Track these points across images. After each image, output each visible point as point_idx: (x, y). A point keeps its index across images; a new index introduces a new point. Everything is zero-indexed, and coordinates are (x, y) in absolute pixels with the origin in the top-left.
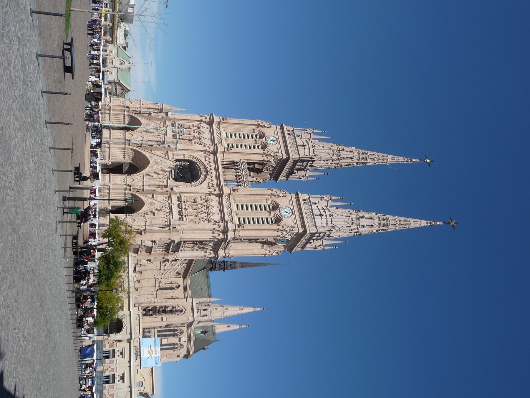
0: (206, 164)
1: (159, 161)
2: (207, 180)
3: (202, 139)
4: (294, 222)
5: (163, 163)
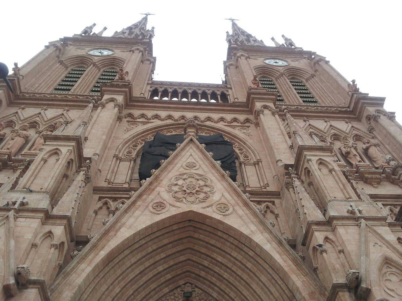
1: (180, 182)
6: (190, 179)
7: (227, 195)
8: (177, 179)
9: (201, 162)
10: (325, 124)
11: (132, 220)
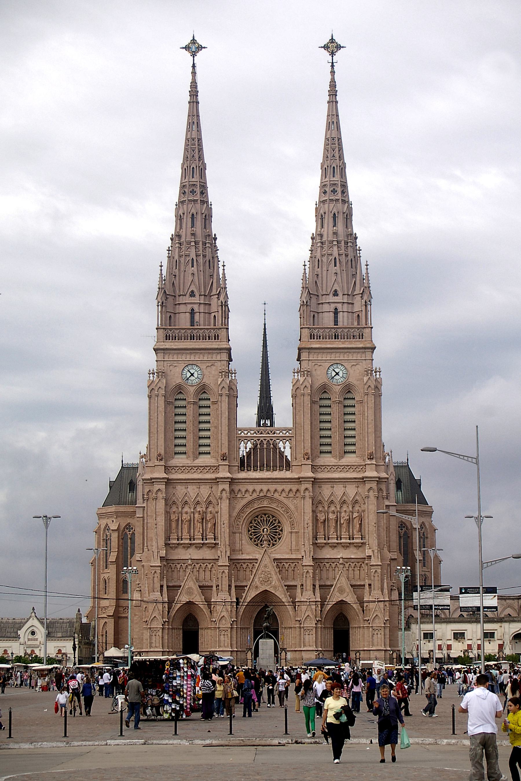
0: (250, 498)
1: (263, 576)
2: (281, 498)
3: (198, 499)
4: (355, 364)
5: (267, 570)
6: (266, 574)
7: (277, 581)
8: (261, 574)
9: (269, 564)
10: (343, 489)
11: (250, 594)
